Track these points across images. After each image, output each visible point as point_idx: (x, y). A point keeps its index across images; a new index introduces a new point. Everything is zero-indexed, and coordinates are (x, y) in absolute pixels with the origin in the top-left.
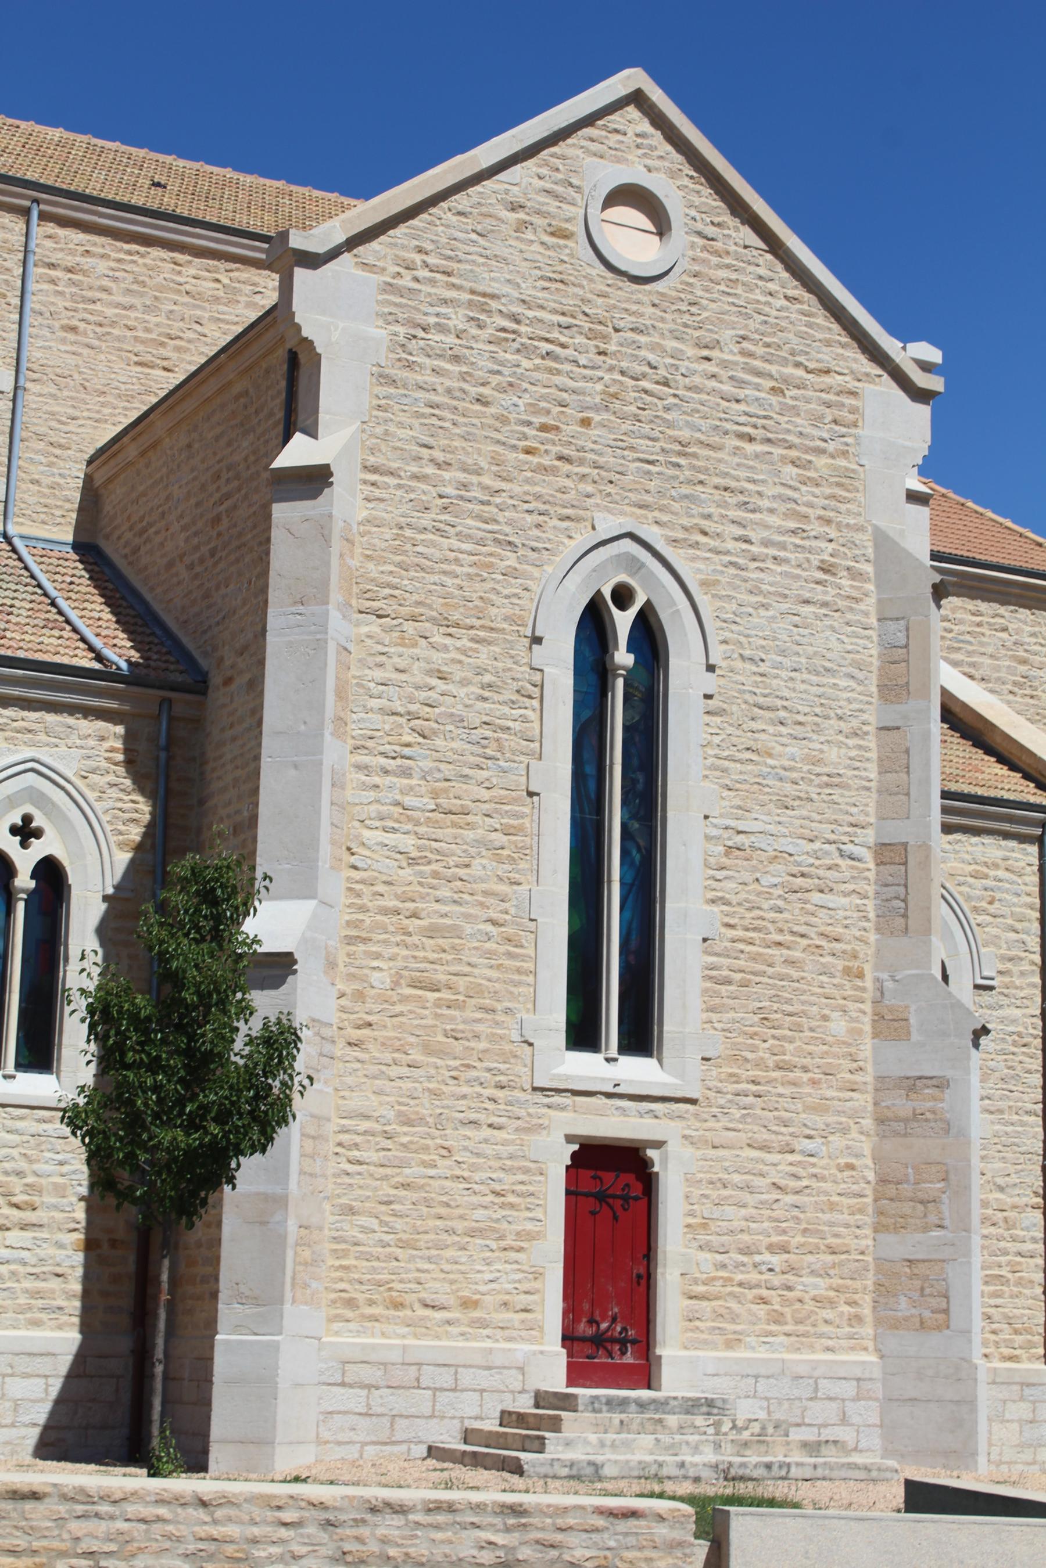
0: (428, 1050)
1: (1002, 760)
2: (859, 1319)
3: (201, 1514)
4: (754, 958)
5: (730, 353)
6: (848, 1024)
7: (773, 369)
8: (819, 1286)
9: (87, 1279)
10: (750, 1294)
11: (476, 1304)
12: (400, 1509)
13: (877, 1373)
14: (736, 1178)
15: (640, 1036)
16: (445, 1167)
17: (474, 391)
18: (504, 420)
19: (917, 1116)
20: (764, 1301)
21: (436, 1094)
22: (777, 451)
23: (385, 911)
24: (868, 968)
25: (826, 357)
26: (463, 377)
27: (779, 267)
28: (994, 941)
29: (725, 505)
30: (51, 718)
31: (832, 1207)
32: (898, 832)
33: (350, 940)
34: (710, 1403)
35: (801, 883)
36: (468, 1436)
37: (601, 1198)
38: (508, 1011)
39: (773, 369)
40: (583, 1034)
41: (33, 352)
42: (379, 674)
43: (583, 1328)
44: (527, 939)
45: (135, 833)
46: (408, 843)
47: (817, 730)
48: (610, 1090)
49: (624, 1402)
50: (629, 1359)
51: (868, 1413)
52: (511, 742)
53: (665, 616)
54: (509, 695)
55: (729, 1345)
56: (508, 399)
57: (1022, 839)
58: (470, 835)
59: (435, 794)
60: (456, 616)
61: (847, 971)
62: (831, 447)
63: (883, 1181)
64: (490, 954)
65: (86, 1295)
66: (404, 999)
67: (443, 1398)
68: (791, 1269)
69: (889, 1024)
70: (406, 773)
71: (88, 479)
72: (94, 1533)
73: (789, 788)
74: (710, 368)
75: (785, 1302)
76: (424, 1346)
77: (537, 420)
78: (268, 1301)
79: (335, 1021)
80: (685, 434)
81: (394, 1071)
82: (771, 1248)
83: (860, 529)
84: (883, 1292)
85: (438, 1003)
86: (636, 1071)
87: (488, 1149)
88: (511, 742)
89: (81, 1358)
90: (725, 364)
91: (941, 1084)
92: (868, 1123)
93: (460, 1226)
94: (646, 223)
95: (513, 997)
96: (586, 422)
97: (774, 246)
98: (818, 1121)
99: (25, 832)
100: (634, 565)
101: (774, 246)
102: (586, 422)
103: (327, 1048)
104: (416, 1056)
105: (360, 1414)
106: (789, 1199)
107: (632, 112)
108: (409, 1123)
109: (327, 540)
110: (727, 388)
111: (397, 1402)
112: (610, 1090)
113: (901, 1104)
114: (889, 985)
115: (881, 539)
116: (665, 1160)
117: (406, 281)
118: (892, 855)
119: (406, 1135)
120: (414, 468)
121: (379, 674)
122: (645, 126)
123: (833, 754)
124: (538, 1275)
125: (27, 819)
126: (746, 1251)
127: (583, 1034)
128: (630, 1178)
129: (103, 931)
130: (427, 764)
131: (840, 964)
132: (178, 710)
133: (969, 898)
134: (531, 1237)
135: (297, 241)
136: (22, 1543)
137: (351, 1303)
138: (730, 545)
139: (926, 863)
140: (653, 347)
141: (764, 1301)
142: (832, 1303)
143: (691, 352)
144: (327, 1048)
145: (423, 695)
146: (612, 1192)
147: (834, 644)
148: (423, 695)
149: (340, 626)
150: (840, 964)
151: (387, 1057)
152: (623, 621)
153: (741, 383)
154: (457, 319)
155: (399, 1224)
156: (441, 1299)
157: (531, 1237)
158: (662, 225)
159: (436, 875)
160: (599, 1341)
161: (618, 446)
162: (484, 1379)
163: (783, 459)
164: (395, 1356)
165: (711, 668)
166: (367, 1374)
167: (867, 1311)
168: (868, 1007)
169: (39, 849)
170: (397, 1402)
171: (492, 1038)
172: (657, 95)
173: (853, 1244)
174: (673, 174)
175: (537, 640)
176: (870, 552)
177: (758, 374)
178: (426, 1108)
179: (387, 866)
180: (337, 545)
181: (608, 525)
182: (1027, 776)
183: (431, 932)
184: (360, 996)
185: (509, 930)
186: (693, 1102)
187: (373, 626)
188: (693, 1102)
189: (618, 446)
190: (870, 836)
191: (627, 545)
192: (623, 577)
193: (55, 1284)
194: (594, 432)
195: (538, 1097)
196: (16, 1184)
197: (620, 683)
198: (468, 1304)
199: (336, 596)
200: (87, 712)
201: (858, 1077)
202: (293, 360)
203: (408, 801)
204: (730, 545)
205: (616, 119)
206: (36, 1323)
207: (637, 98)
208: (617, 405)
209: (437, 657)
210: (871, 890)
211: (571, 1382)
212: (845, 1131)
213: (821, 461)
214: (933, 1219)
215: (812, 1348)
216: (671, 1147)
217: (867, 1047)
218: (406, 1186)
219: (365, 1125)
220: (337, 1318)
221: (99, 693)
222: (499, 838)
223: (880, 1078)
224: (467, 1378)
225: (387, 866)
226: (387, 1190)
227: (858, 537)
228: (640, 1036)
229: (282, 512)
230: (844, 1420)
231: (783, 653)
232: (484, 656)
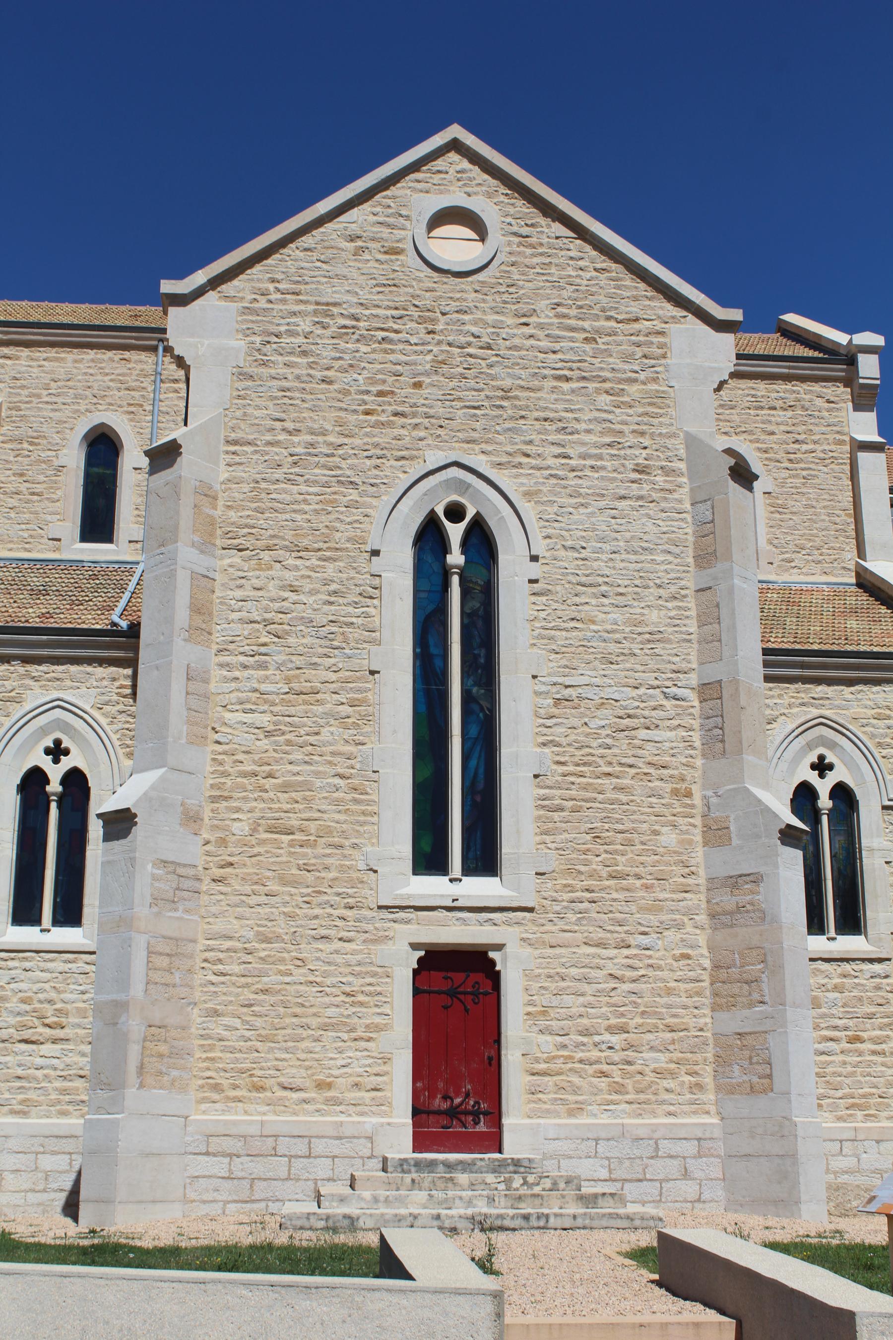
0: (284, 881)
2: (700, 1086)
4: (585, 788)
5: (546, 317)
6: (679, 839)
7: (586, 324)
8: (661, 1060)
10: (590, 1070)
11: (329, 1086)
13: (717, 1133)
14: (574, 971)
15: (484, 858)
16: (300, 974)
17: (319, 375)
18: (346, 393)
19: (740, 908)
20: (604, 1074)
21: (291, 916)
22: (591, 386)
23: (244, 775)
24: (696, 790)
25: (634, 309)
26: (310, 366)
27: (588, 248)
29: (546, 432)
30: (74, 669)
31: (669, 992)
32: (715, 672)
33: (214, 799)
35: (627, 724)
37: (453, 994)
38: (355, 846)
39: (586, 324)
42: (239, 594)
43: (438, 1103)
44: (369, 787)
46: (264, 720)
47: (638, 597)
48: (455, 905)
49: (432, 1164)
50: (482, 1127)
52: (354, 634)
53: (492, 523)
54: (352, 598)
55: (571, 1113)
56: (348, 378)
58: (320, 709)
60: (305, 542)
61: (675, 792)
62: (642, 376)
63: (716, 967)
64: (337, 802)
67: (298, 1164)
68: (631, 1046)
69: (716, 834)
70: (263, 666)
73: (613, 647)
74: (527, 330)
75: (625, 1074)
76: (277, 1120)
77: (374, 389)
79: (200, 862)
80: (507, 383)
82: (610, 1029)
83: (674, 435)
84: (722, 1062)
85: (291, 844)
87: (339, 959)
88: (354, 634)
90: (541, 326)
91: (756, 879)
92: (702, 918)
93: (314, 1022)
94: (472, 235)
95: (359, 834)
98: (653, 919)
99: (57, 752)
102: (418, 385)
103: (187, 884)
104: (273, 887)
105: (223, 1178)
106: (627, 987)
107: (453, 156)
108: (268, 941)
110: (544, 344)
111: (257, 1167)
112: (455, 905)
113: (728, 900)
114: (714, 800)
115: (691, 441)
116: (504, 960)
117: (263, 304)
118: (710, 691)
120: (268, 437)
121: (239, 594)
122: (465, 164)
123: (654, 616)
124: (386, 1060)
126: (586, 1033)
128: (479, 977)
130: (280, 658)
131: (668, 787)
133: (872, 736)
134: (378, 1028)
137: (217, 1088)
138: (551, 462)
139: (735, 695)
140: (475, 323)
141: (604, 1074)
142: (673, 1075)
143: (510, 321)
144: (187, 884)
145: (277, 606)
146: (457, 992)
147: (649, 527)
148: (277, 606)
150: (668, 787)
151: (248, 889)
152: (455, 532)
153: (557, 339)
154: (305, 325)
155: (258, 1022)
156: (298, 1082)
157: (378, 1028)
158: (482, 233)
159: (289, 743)
160: (454, 1113)
161: (448, 398)
162: (335, 1147)
163: (598, 391)
164: (254, 1130)
165: (534, 558)
166: (228, 1145)
167: (708, 1080)
168: (698, 821)
169: (66, 764)
170: (257, 1167)
171: (341, 869)
172: (471, 140)
173: (691, 1022)
174: (489, 195)
175: (376, 553)
176: (682, 452)
177: (573, 329)
178: (282, 927)
179: (245, 739)
181: (435, 458)
183: (285, 788)
184: (222, 842)
185: (355, 782)
186: (530, 910)
187: (236, 558)
188: (530, 910)
189: (448, 398)
190: (693, 679)
191: (455, 472)
192: (455, 497)
194: (425, 392)
195: (385, 914)
196: (49, 1010)
197: (455, 580)
198: (321, 1086)
201: (690, 881)
203: (263, 687)
204: (551, 462)
205: (439, 164)
206: (64, 1113)
207: (455, 145)
208: (445, 369)
209: (288, 575)
210: (696, 724)
211: (416, 1149)
212: (680, 926)
213: (633, 389)
214: (756, 996)
215: (654, 1114)
216: (508, 949)
217: (699, 854)
218: (265, 991)
219: (228, 944)
220: (204, 1100)
222: (345, 710)
223: (710, 880)
224: (319, 1147)
225: (245, 739)
227: (670, 443)
228: (484, 858)
230: (686, 1175)
231: (602, 540)
232: (330, 569)
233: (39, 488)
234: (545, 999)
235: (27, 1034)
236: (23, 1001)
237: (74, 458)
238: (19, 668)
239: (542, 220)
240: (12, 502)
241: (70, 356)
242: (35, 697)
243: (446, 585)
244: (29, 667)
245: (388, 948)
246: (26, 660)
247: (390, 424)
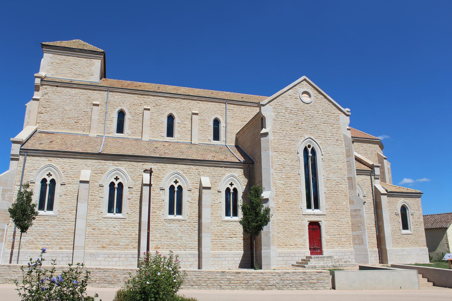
0: (288, 210)
1: (364, 164)
3: (262, 275)
4: (332, 194)
6: (346, 203)
8: (345, 239)
9: (244, 244)
12: (289, 273)
19: (356, 215)
20: (337, 242)
23: (280, 192)
25: (334, 111)
26: (285, 119)
28: (365, 190)
30: (234, 169)
31: (346, 228)
33: (276, 196)
34: (330, 257)
35: (338, 183)
36: (297, 263)
37: (313, 229)
40: (309, 207)
41: (227, 121)
42: (277, 160)
43: (312, 247)
45: (246, 184)
46: (283, 182)
48: (313, 214)
49: (319, 257)
50: (319, 251)
51: (353, 257)
55: (333, 248)
57: (368, 175)
59: (286, 175)
61: (345, 195)
63: (352, 224)
64: (295, 197)
65: (244, 246)
66: (284, 204)
68: (341, 237)
69: (352, 202)
70: (282, 173)
71: (236, 137)
72: (248, 278)
74: (318, 114)
78: (269, 246)
80: (316, 124)
81: (283, 213)
82: (337, 235)
85: (289, 204)
86: (317, 211)
89: (244, 255)
90: (320, 114)
91: (359, 210)
92: (350, 216)
93: (294, 234)
94: (307, 96)
96: (302, 123)
97: (325, 97)
98: (343, 216)
100: (310, 142)
101: (325, 97)
102: (302, 123)
107: (304, 82)
109: (268, 142)
111: (287, 259)
112: (313, 214)
113: (354, 213)
115: (344, 135)
118: (350, 179)
119: (286, 222)
121: (277, 160)
122: (306, 83)
123: (340, 165)
124: (305, 240)
125: (231, 183)
126: (334, 235)
127: (309, 207)
128: (317, 226)
129: (242, 197)
132: (250, 167)
134: (304, 235)
135: (261, 103)
136: (238, 279)
137: (280, 245)
139: (355, 179)
140: (310, 112)
149: (271, 153)
152: (310, 150)
153: (323, 116)
154: (283, 111)
155: (285, 234)
156: (292, 244)
157: (304, 235)
158: (310, 96)
160: (314, 249)
162: (299, 255)
164: (286, 252)
165: (322, 155)
166: (283, 255)
167: (352, 243)
169: (233, 187)
170: (287, 259)
171: (296, 208)
172: (307, 79)
174: (311, 89)
175: (298, 153)
180: (270, 143)
181: (307, 137)
182: (368, 166)
183: (287, 194)
184: (278, 203)
187: (276, 153)
190: (346, 176)
192: (309, 144)
193: (240, 245)
196: (234, 232)
198: (296, 245)
199: (270, 150)
200: (238, 168)
202: (262, 119)
205: (302, 83)
206: (238, 250)
207: (305, 80)
210: (347, 184)
212: (347, 218)
213: (335, 125)
216: (322, 222)
217: (349, 206)
221: (240, 165)
222: (295, 181)
224: (296, 255)
226: (283, 230)
229: (262, 139)
230: (349, 258)
232: (291, 156)
233: (206, 130)
234: (328, 230)
235: (230, 236)
236: (230, 230)
237: (211, 124)
238: (224, 169)
239: (319, 94)
240: (201, 132)
241: (210, 103)
242: (228, 174)
243: (308, 159)
244: (226, 169)
245: (304, 221)
246: (225, 167)
247: (298, 130)
